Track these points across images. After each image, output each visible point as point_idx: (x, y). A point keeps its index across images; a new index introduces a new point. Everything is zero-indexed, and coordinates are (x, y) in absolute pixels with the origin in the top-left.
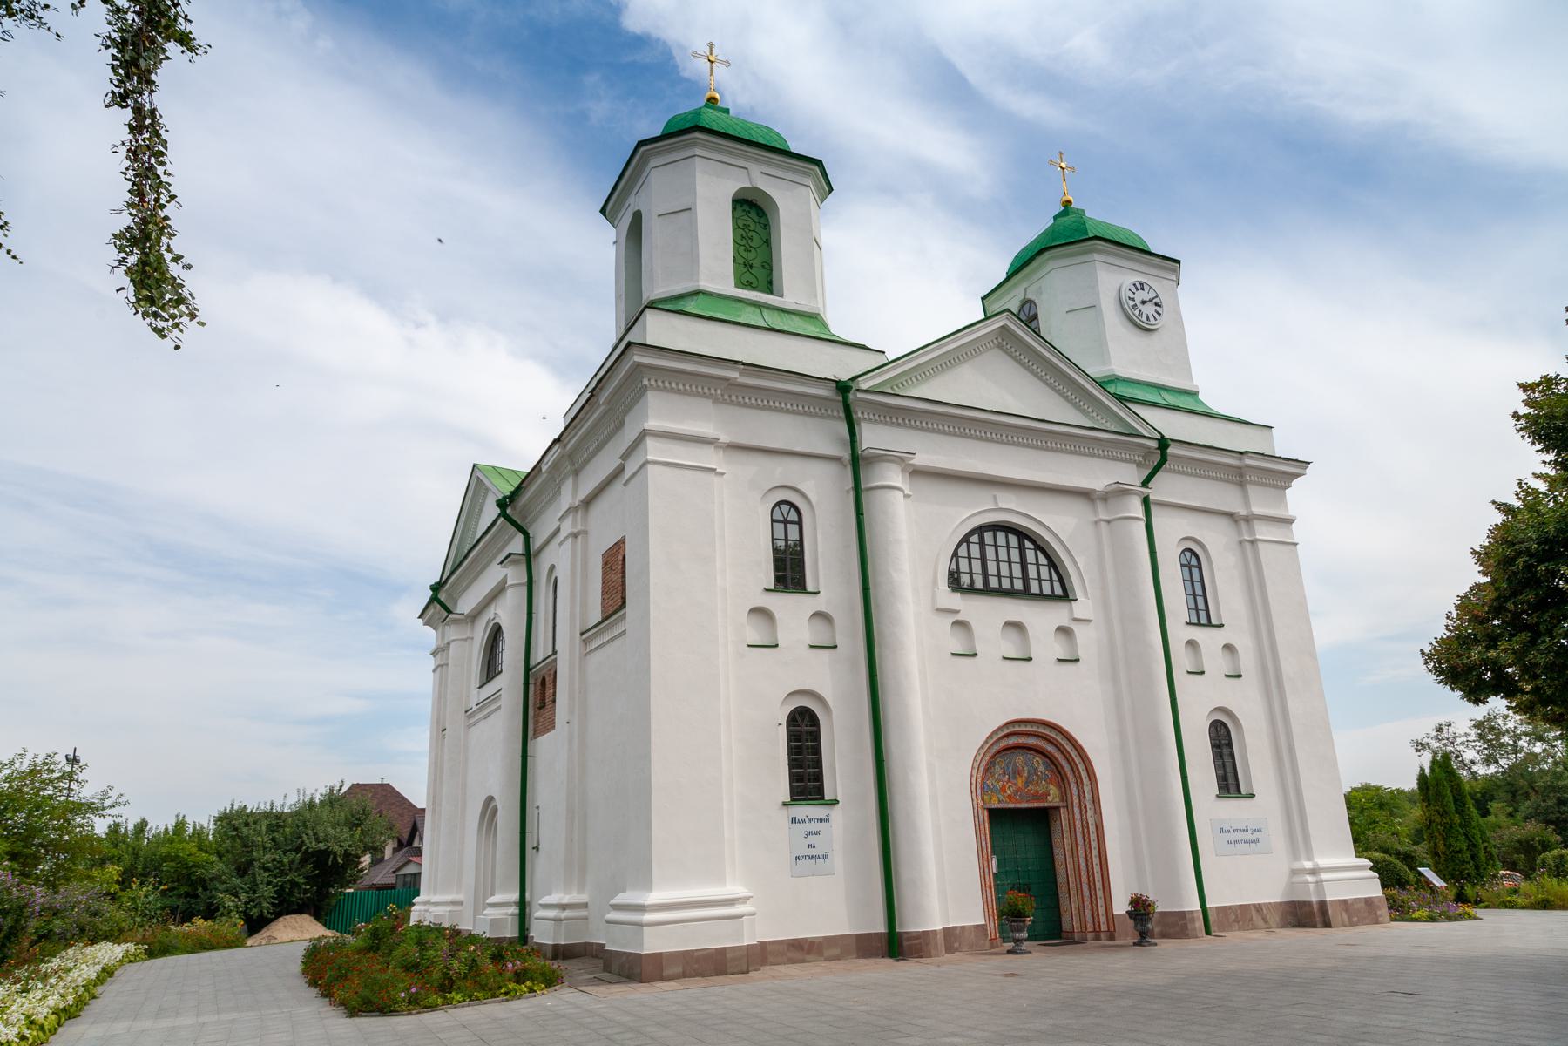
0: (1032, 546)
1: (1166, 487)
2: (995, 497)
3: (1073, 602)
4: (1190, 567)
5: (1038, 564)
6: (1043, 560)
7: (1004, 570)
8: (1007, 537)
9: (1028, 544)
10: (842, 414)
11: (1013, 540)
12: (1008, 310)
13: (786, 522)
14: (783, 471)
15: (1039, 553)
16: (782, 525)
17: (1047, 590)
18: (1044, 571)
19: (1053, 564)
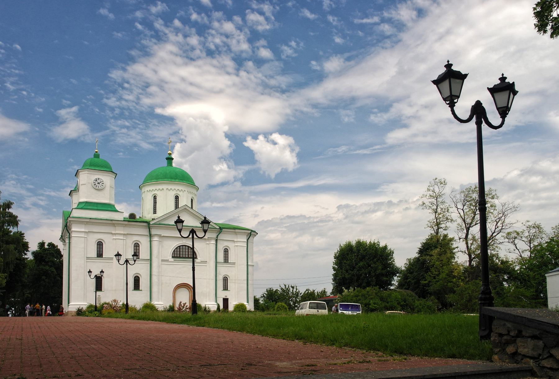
1: (222, 236)
4: (226, 251)
7: (184, 253)
9: (189, 248)
11: (187, 248)
13: (136, 246)
14: (136, 238)
16: (136, 247)
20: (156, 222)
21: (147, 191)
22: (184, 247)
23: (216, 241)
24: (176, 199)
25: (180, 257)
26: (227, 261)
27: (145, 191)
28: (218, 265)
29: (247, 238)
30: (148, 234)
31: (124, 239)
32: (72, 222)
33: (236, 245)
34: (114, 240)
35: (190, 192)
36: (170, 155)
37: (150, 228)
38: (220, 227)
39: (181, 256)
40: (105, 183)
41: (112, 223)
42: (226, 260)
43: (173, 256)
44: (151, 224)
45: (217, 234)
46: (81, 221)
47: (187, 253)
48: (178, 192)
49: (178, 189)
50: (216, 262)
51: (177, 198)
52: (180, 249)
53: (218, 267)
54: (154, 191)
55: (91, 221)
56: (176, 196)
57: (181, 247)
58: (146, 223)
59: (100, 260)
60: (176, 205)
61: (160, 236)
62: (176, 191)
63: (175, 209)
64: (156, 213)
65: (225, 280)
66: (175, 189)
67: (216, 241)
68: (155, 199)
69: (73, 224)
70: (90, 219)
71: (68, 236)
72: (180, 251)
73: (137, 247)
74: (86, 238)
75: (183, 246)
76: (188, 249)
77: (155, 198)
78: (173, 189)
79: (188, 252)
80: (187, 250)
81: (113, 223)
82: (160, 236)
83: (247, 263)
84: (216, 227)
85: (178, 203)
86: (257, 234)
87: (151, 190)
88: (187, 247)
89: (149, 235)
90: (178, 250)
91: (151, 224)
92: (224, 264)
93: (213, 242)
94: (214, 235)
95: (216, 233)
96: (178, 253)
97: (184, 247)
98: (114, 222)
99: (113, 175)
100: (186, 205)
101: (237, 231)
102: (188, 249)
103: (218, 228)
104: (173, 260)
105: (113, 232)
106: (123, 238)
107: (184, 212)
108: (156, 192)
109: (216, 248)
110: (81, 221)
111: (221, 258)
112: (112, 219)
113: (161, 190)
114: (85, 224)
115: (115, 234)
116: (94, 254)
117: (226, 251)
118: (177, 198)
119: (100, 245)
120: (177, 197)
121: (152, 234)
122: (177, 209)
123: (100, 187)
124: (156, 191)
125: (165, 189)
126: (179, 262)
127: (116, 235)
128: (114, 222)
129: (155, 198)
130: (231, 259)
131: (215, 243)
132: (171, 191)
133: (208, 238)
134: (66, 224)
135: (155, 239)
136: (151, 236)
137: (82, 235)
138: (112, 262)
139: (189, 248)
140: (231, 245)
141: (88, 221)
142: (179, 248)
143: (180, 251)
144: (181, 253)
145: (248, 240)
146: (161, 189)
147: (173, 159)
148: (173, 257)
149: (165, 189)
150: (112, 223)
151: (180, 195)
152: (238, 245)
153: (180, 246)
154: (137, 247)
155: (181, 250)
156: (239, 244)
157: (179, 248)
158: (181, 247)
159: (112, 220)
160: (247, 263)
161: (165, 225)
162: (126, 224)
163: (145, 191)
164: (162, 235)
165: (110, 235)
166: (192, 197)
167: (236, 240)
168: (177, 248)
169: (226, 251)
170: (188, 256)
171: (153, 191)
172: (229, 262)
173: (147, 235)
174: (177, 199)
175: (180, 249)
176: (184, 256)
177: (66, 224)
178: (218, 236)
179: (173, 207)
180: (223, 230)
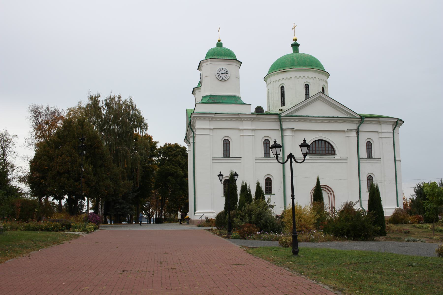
0: (327, 143)
1: (364, 127)
2: (318, 134)
3: (335, 156)
5: (328, 147)
6: (330, 146)
7: (320, 149)
8: (322, 141)
9: (326, 143)
10: (279, 120)
11: (323, 142)
12: (320, 92)
13: (267, 143)
15: (329, 145)
17: (330, 152)
18: (330, 149)
19: (332, 147)
20: (287, 113)
21: (274, 81)
22: (320, 142)
23: (358, 132)
24: (306, 88)
26: (371, 156)
27: (271, 82)
28: (360, 162)
29: (393, 127)
30: (279, 128)
31: (252, 135)
32: (196, 119)
33: (381, 137)
34: (241, 136)
35: (321, 79)
37: (281, 121)
38: (361, 117)
39: (317, 152)
40: (229, 74)
41: (239, 117)
42: (370, 155)
44: (282, 116)
45: (358, 125)
46: (205, 117)
47: (324, 149)
48: (308, 80)
50: (359, 159)
51: (307, 86)
52: (315, 144)
53: (360, 164)
54: (282, 80)
56: (305, 85)
57: (317, 142)
58: (277, 116)
59: (227, 160)
60: (307, 95)
61: (293, 130)
62: (306, 79)
63: (306, 100)
64: (284, 105)
65: (370, 179)
67: (358, 132)
68: (282, 90)
69: (197, 121)
70: (215, 113)
71: (192, 136)
72: (316, 147)
73: (267, 144)
74: (211, 136)
76: (325, 144)
77: (282, 88)
78: (302, 77)
79: (325, 147)
80: (323, 146)
81: (241, 118)
82: (293, 130)
83: (395, 158)
84: (357, 116)
85: (309, 92)
86: (403, 122)
87: (278, 80)
88: (324, 142)
89: (280, 130)
90: (314, 145)
91: (282, 116)
92: (368, 160)
93: (355, 134)
94: (355, 126)
95: (357, 123)
98: (241, 116)
101: (381, 120)
103: (359, 117)
104: (308, 158)
105: (241, 128)
106: (251, 134)
108: (283, 82)
109: (358, 141)
110: (205, 117)
111: (363, 153)
112: (239, 113)
113: (289, 79)
114: (210, 120)
115: (243, 130)
116: (220, 153)
117: (369, 145)
118: (307, 86)
119: (226, 143)
120: (306, 85)
121: (284, 128)
122: (307, 99)
123: (222, 78)
124: (284, 80)
125: (293, 77)
126: (315, 160)
127: (244, 130)
128: (241, 116)
129: (282, 88)
130: (375, 154)
131: (356, 135)
132: (300, 79)
133: (348, 129)
134: (190, 122)
136: (282, 130)
137: (208, 132)
138: (241, 162)
140: (374, 138)
141: (213, 116)
142: (314, 143)
143: (316, 147)
144: (317, 149)
145: (393, 130)
146: (289, 78)
147: (300, 45)
149: (293, 77)
150: (239, 117)
151: (310, 83)
152: (383, 137)
153: (315, 141)
154: (267, 144)
155: (317, 145)
156: (384, 135)
157: (314, 143)
158: (316, 141)
159: (239, 114)
160: (395, 158)
161: (298, 116)
162: (255, 118)
163: (271, 82)
164: (295, 129)
165: (237, 131)
166: (324, 85)
167: (380, 131)
169: (369, 145)
170: (325, 152)
171: (280, 81)
172: (373, 157)
173: (278, 130)
174: (308, 88)
175: (315, 144)
176: (321, 153)
177: (190, 122)
179: (304, 98)
180: (365, 119)
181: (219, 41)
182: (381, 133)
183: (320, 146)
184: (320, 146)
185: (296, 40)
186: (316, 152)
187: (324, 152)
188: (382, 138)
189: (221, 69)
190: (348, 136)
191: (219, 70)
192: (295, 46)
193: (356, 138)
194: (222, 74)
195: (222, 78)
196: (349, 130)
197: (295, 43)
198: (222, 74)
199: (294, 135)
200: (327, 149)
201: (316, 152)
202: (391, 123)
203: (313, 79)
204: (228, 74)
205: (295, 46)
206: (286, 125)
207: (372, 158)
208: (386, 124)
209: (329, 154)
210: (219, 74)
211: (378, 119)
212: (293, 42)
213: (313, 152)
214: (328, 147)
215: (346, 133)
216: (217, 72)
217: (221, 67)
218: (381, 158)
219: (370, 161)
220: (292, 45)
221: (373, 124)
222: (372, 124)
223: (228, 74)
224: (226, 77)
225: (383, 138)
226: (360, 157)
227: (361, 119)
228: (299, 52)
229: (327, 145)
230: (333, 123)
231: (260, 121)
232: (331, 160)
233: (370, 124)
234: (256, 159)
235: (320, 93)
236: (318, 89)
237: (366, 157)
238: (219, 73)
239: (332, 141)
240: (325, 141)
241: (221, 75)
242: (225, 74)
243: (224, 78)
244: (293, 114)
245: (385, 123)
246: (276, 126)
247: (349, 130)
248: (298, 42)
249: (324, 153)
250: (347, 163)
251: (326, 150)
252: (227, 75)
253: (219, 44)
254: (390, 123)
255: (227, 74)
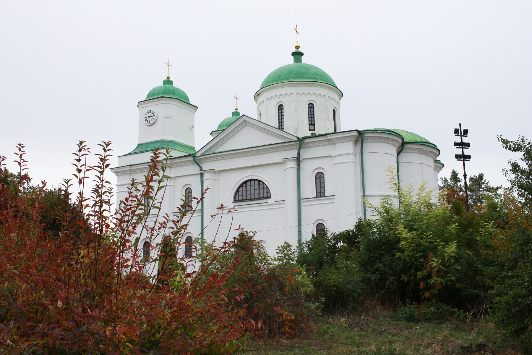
0: (262, 183)
7: (253, 192)
11: (257, 182)
14: (186, 180)
18: (265, 190)
25: (247, 200)
28: (302, 204)
33: (334, 163)
36: (297, 49)
38: (298, 138)
40: (156, 116)
42: (320, 193)
43: (237, 198)
47: (257, 192)
49: (319, 94)
50: (299, 200)
52: (246, 186)
55: (132, 168)
56: (309, 104)
57: (249, 183)
58: (191, 157)
66: (281, 95)
72: (246, 191)
75: (250, 180)
76: (259, 184)
79: (259, 189)
80: (257, 187)
83: (364, 192)
90: (244, 188)
93: (292, 164)
94: (294, 154)
96: (244, 193)
97: (253, 182)
99: (171, 101)
100: (243, 115)
102: (259, 184)
107: (247, 126)
117: (320, 178)
135: (206, 176)
139: (261, 183)
141: (129, 169)
143: (246, 191)
144: (249, 192)
148: (235, 201)
153: (246, 182)
155: (249, 188)
157: (244, 185)
160: (364, 192)
168: (241, 186)
169: (320, 178)
170: (259, 195)
176: (253, 197)
178: (299, 154)
181: (168, 78)
182: (335, 156)
183: (253, 187)
184: (253, 187)
185: (298, 48)
186: (246, 197)
187: (257, 196)
188: (335, 164)
189: (149, 112)
190: (285, 169)
191: (147, 113)
192: (297, 55)
193: (295, 171)
194: (149, 117)
195: (149, 122)
196: (284, 161)
197: (297, 51)
198: (149, 117)
199: (216, 178)
200: (261, 191)
201: (246, 197)
202: (348, 140)
203: (289, 96)
204: (154, 116)
205: (297, 55)
206: (206, 166)
207: (325, 196)
208: (341, 142)
209: (264, 198)
210: (146, 119)
211: (325, 136)
212: (294, 50)
213: (251, 197)
214: (263, 188)
215: (284, 164)
216: (144, 116)
217: (148, 109)
218: (334, 196)
219: (321, 201)
220: (293, 54)
221: (323, 145)
222: (321, 146)
223: (154, 116)
224: (153, 120)
225: (337, 165)
226: (302, 196)
227: (299, 142)
228: (303, 62)
229: (261, 186)
230: (264, 153)
231: (179, 166)
232: (264, 206)
233: (317, 146)
234: (174, 214)
235: (244, 116)
236: (296, 109)
237: (315, 196)
238: (146, 117)
239: (265, 179)
240: (259, 181)
241: (148, 119)
242: (152, 116)
243: (151, 122)
244: (214, 151)
245: (339, 141)
246: (195, 169)
247: (284, 161)
248: (300, 50)
249: (258, 197)
250: (284, 207)
251: (259, 193)
252: (154, 117)
253: (168, 82)
254: (346, 140)
255: (154, 116)
